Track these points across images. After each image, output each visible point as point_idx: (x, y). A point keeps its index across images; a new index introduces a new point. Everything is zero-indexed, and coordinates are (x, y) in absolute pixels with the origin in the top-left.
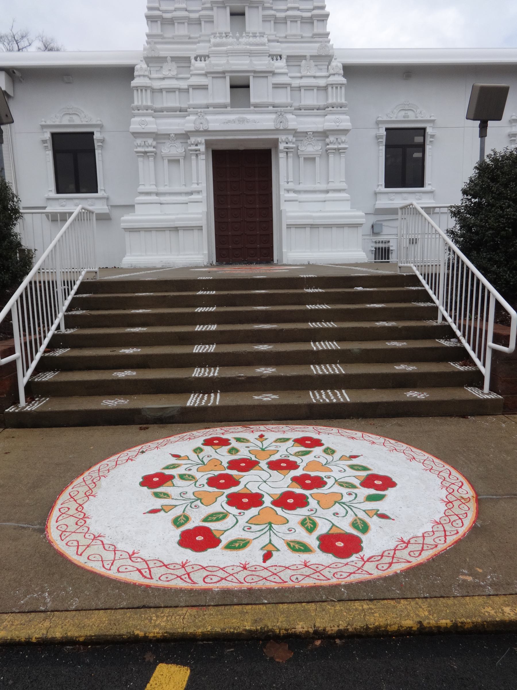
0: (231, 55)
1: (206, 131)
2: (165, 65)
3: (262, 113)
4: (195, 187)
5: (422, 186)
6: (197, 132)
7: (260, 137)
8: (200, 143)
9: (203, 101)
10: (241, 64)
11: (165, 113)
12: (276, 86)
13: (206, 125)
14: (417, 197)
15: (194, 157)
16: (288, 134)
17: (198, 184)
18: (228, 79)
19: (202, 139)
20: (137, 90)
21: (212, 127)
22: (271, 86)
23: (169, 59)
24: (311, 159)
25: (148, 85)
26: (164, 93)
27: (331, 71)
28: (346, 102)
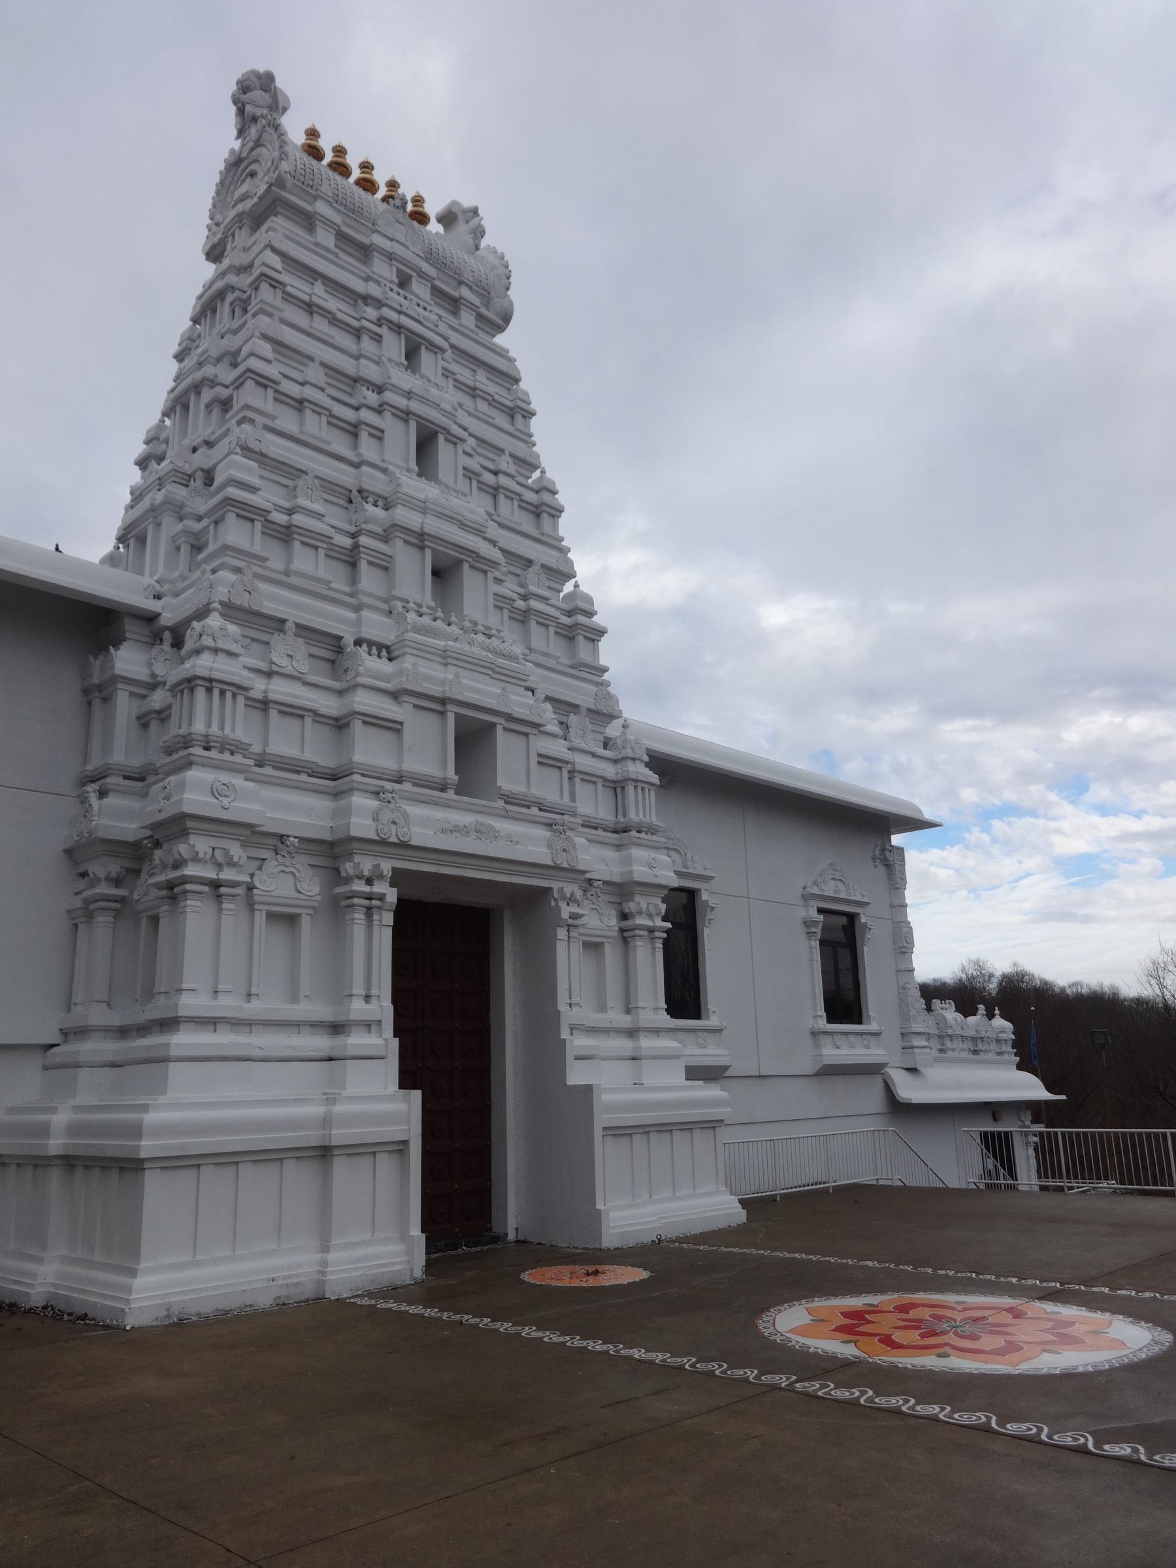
0: (455, 662)
1: (404, 845)
2: (276, 640)
3: (517, 819)
4: (358, 1008)
5: (698, 1016)
6: (382, 844)
7: (515, 880)
8: (381, 877)
9: (389, 764)
10: (481, 691)
11: (268, 770)
12: (546, 761)
13: (406, 830)
14: (700, 1041)
15: (359, 916)
16: (572, 881)
17: (367, 998)
18: (451, 718)
19: (387, 867)
20: (209, 690)
21: (420, 836)
22: (534, 759)
23: (289, 625)
24: (593, 947)
25: (245, 683)
26: (273, 713)
27: (630, 754)
28: (661, 824)
